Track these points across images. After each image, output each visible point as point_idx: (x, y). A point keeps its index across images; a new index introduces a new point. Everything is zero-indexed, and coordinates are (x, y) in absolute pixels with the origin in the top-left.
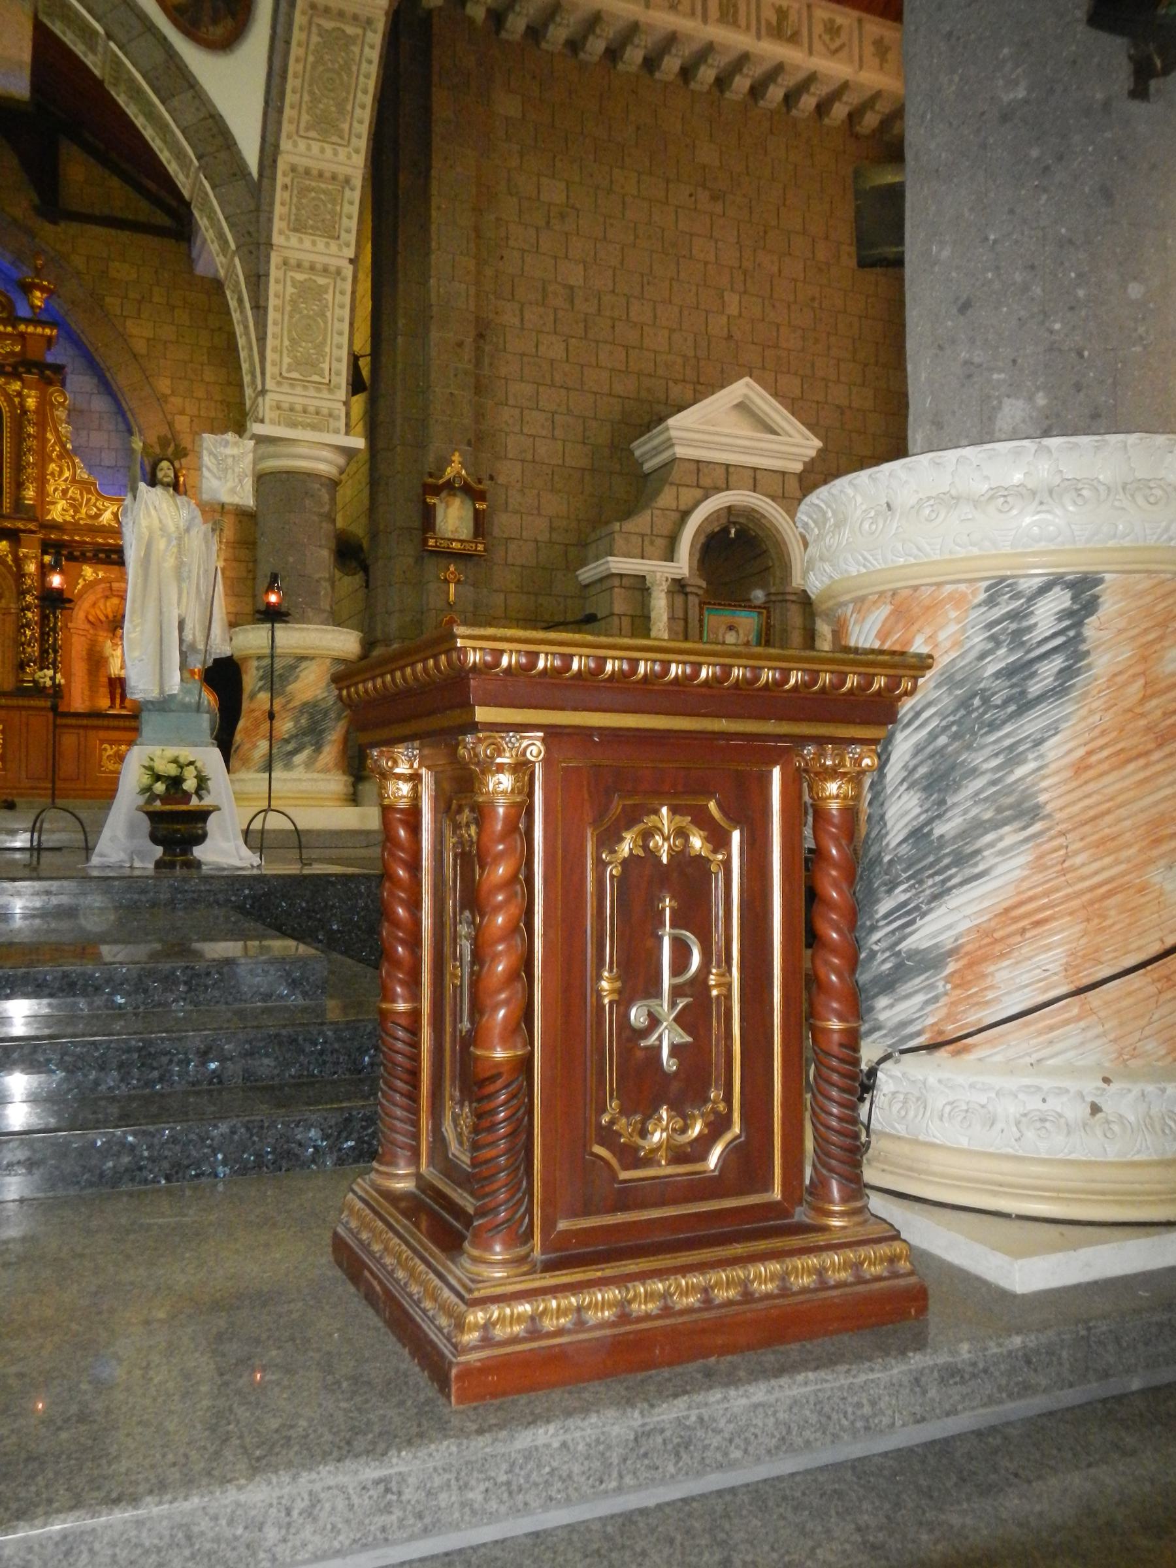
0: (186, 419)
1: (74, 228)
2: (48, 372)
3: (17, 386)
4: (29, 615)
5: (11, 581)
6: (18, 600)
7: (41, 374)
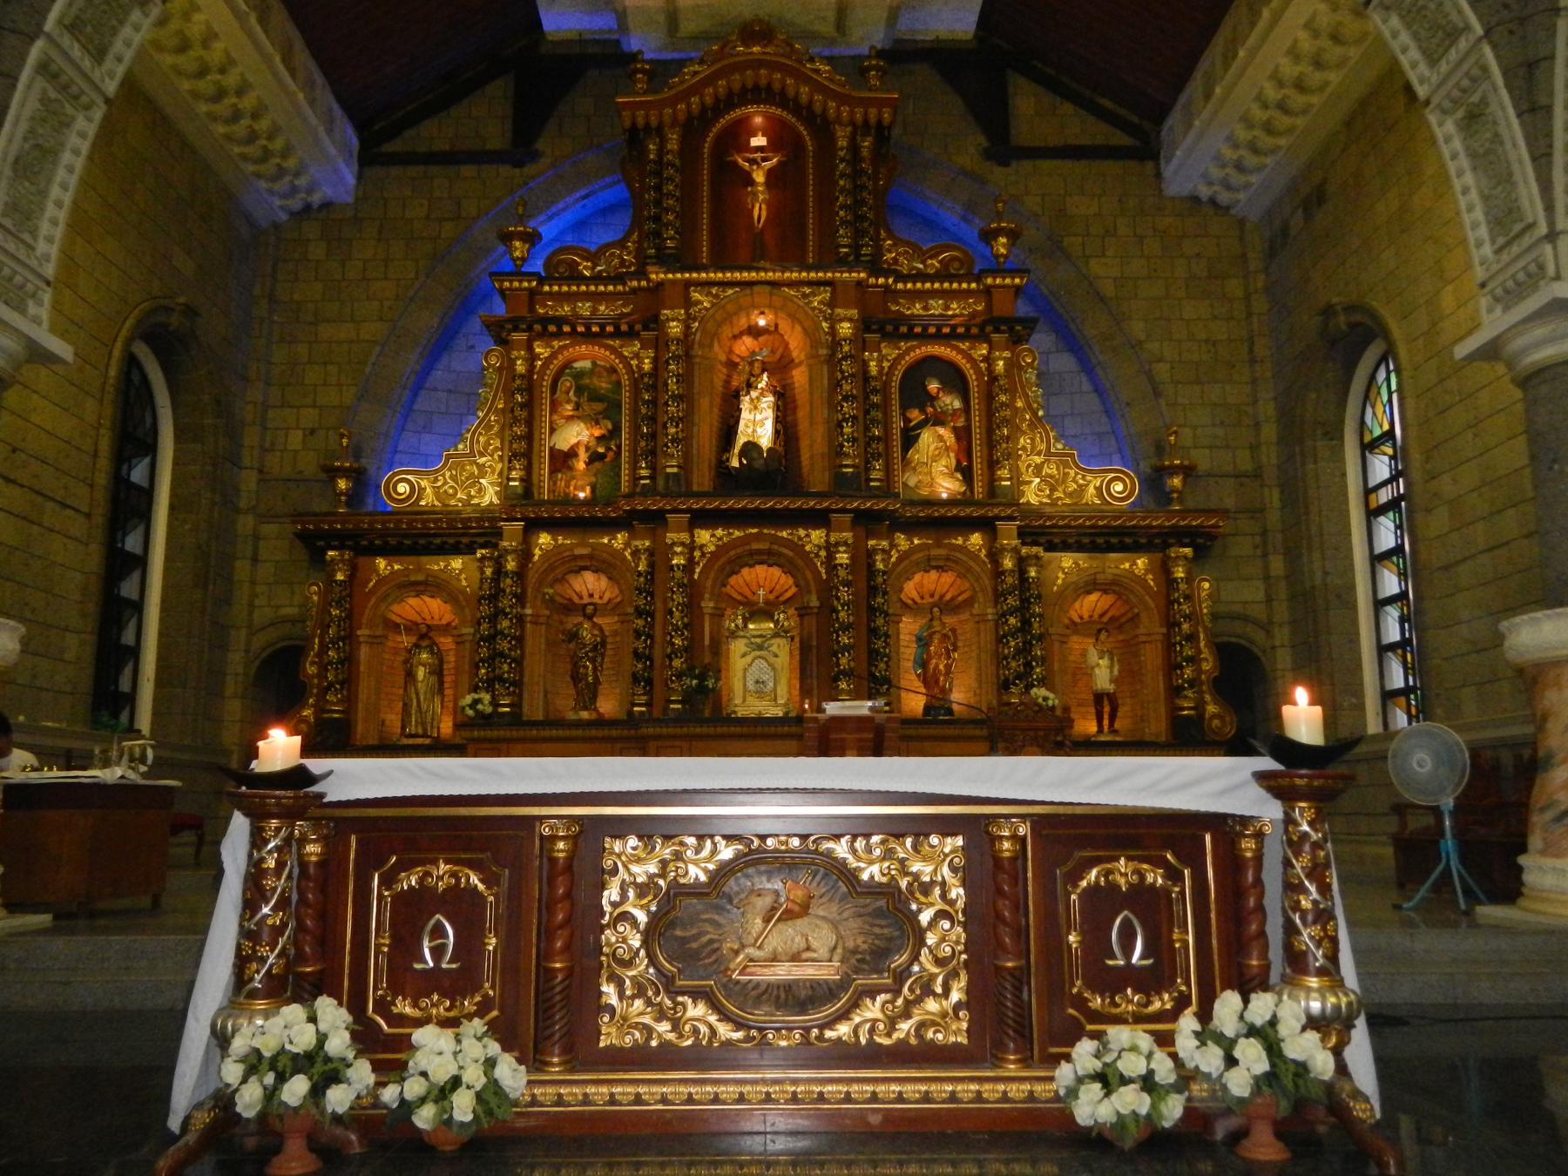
0: (1168, 366)
1: (1027, 165)
2: (1018, 328)
3: (984, 350)
4: (1012, 621)
5: (987, 581)
6: (996, 606)
7: (1011, 329)
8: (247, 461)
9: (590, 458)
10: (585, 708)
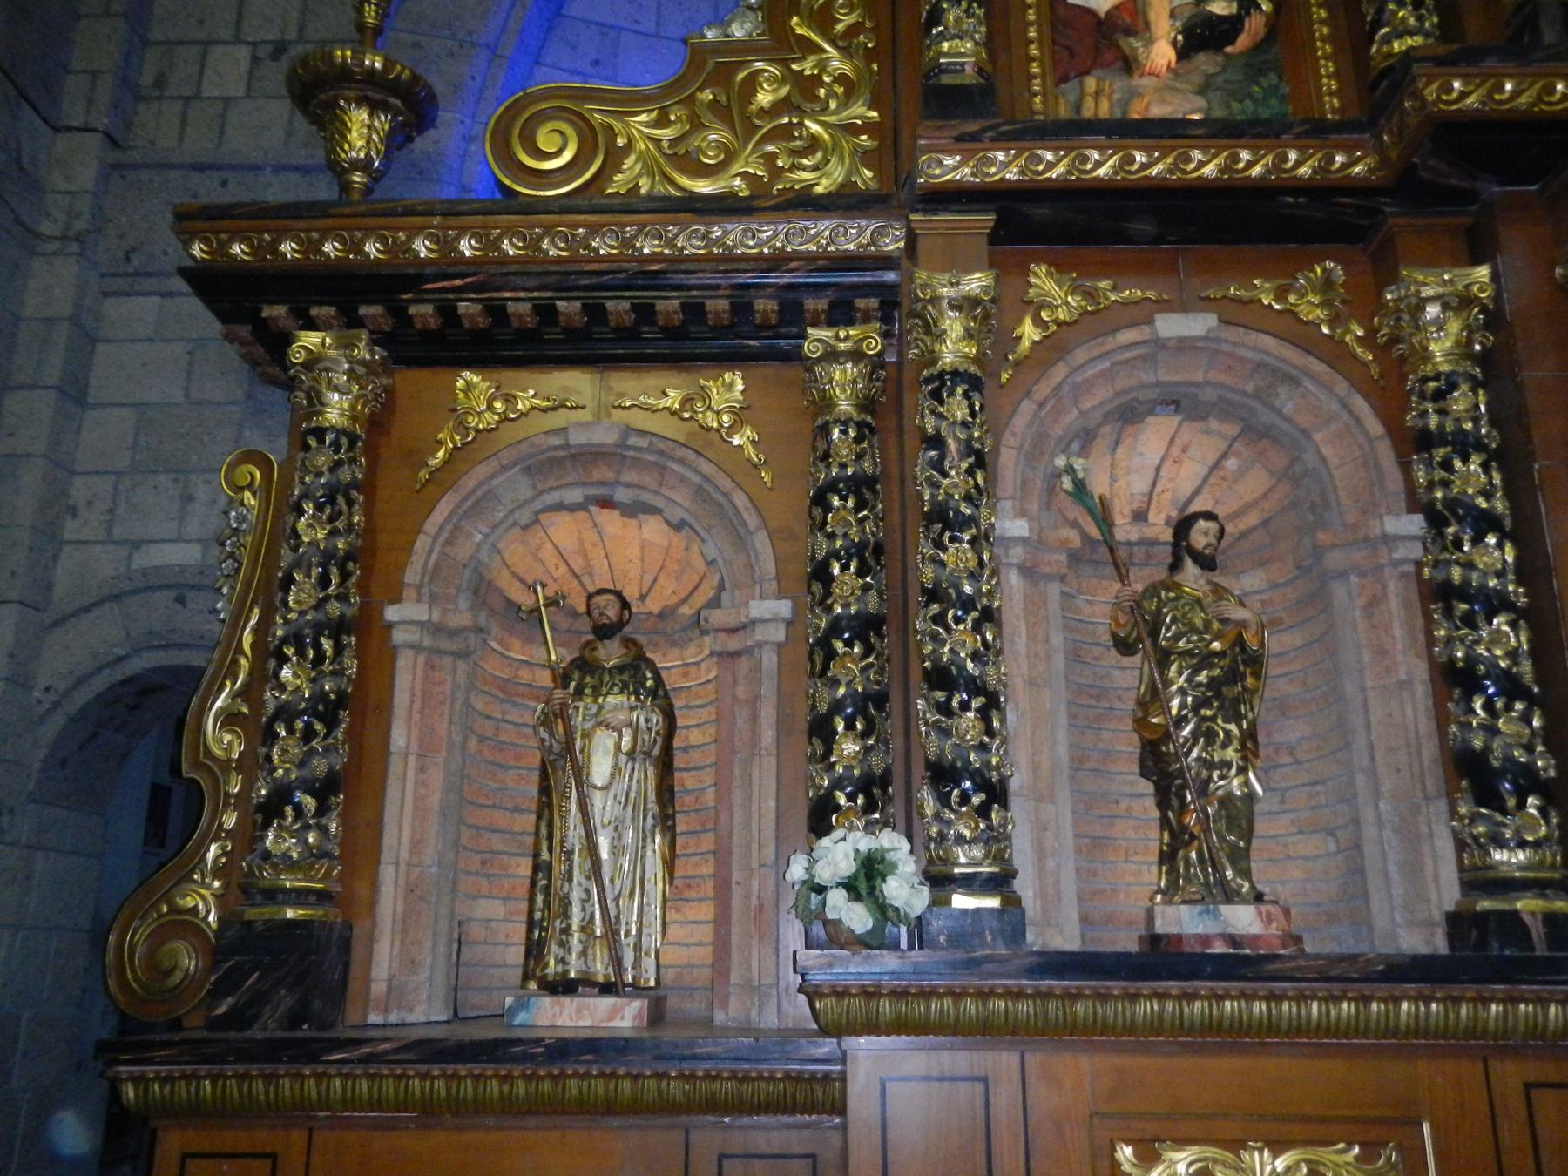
8: (74, 112)
9: (1187, 31)
10: (1231, 896)
